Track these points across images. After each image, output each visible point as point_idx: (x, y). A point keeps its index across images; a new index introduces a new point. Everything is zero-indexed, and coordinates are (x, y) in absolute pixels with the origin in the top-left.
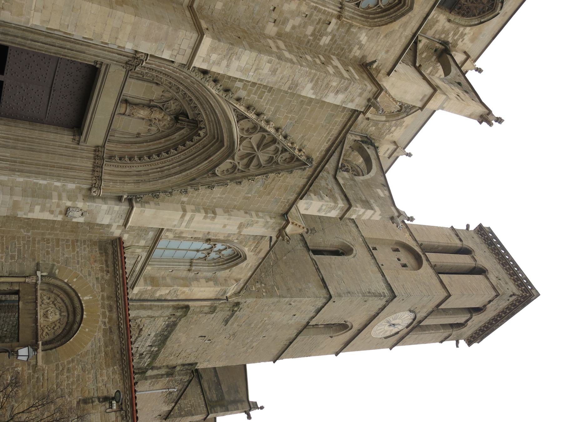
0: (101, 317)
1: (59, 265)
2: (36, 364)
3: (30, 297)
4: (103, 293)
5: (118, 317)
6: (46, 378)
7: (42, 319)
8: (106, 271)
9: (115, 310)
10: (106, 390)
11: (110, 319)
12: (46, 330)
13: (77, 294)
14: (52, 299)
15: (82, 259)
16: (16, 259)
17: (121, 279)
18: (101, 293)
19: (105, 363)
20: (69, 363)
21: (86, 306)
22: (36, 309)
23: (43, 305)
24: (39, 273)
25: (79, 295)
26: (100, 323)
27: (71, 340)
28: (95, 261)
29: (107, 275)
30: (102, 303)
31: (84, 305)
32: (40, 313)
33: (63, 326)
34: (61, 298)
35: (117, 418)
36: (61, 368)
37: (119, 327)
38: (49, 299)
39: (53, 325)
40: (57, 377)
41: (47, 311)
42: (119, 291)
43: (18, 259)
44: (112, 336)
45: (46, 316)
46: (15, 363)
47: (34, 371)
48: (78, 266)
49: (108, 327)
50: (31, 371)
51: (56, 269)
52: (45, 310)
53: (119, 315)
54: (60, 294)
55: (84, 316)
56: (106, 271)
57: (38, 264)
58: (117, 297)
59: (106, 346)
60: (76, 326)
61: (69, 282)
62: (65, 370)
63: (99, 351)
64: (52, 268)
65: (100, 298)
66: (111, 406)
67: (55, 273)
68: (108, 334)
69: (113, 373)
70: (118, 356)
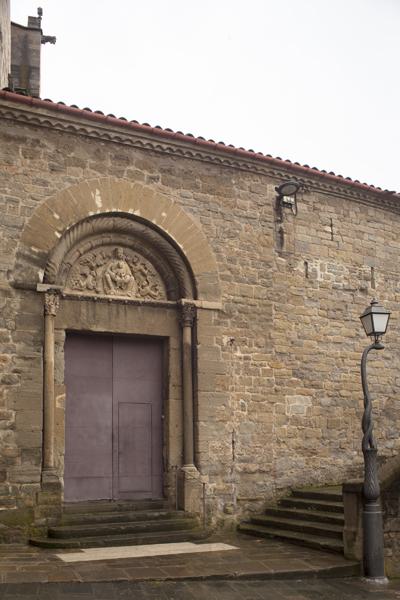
0: (141, 183)
1: (19, 243)
2: (218, 310)
3: (84, 310)
4: (88, 165)
5: (142, 149)
6: (241, 299)
7: (128, 292)
8: (33, 145)
9: (126, 152)
10: (265, 207)
11: (146, 167)
12: (148, 288)
13: (89, 219)
14: (86, 270)
15: (5, 192)
16: (5, 330)
17: (63, 117)
18: (88, 169)
19: (225, 196)
20: (220, 258)
21: (116, 205)
22: (109, 302)
23: (100, 289)
24: (41, 288)
25: (91, 214)
26: (150, 187)
27: (181, 246)
28: (9, 163)
29: (43, 146)
30: (111, 172)
31: (114, 210)
32: (115, 294)
33: (141, 257)
34: (85, 253)
35: (304, 201)
36: (229, 273)
37: (163, 154)
38: (85, 276)
39: (139, 274)
40: (240, 281)
41: (114, 282)
42: (89, 130)
43: (6, 327)
44: (177, 172)
45: (123, 286)
46: (216, 345)
47: (230, 315)
48: (21, 204)
49: (160, 175)
50: (229, 321)
51: (31, 251)
52: (111, 285)
53: (139, 145)
54: (77, 253)
55: (137, 213)
56: (33, 145)
57: (17, 286)
58: (98, 139)
59: (196, 187)
60: (153, 234)
61: (61, 229)
62: (232, 266)
63: (205, 202)
64: (28, 259)
65: (99, 174)
66: (289, 205)
67: (39, 254)
68: (173, 178)
69: (242, 188)
70: (215, 171)
